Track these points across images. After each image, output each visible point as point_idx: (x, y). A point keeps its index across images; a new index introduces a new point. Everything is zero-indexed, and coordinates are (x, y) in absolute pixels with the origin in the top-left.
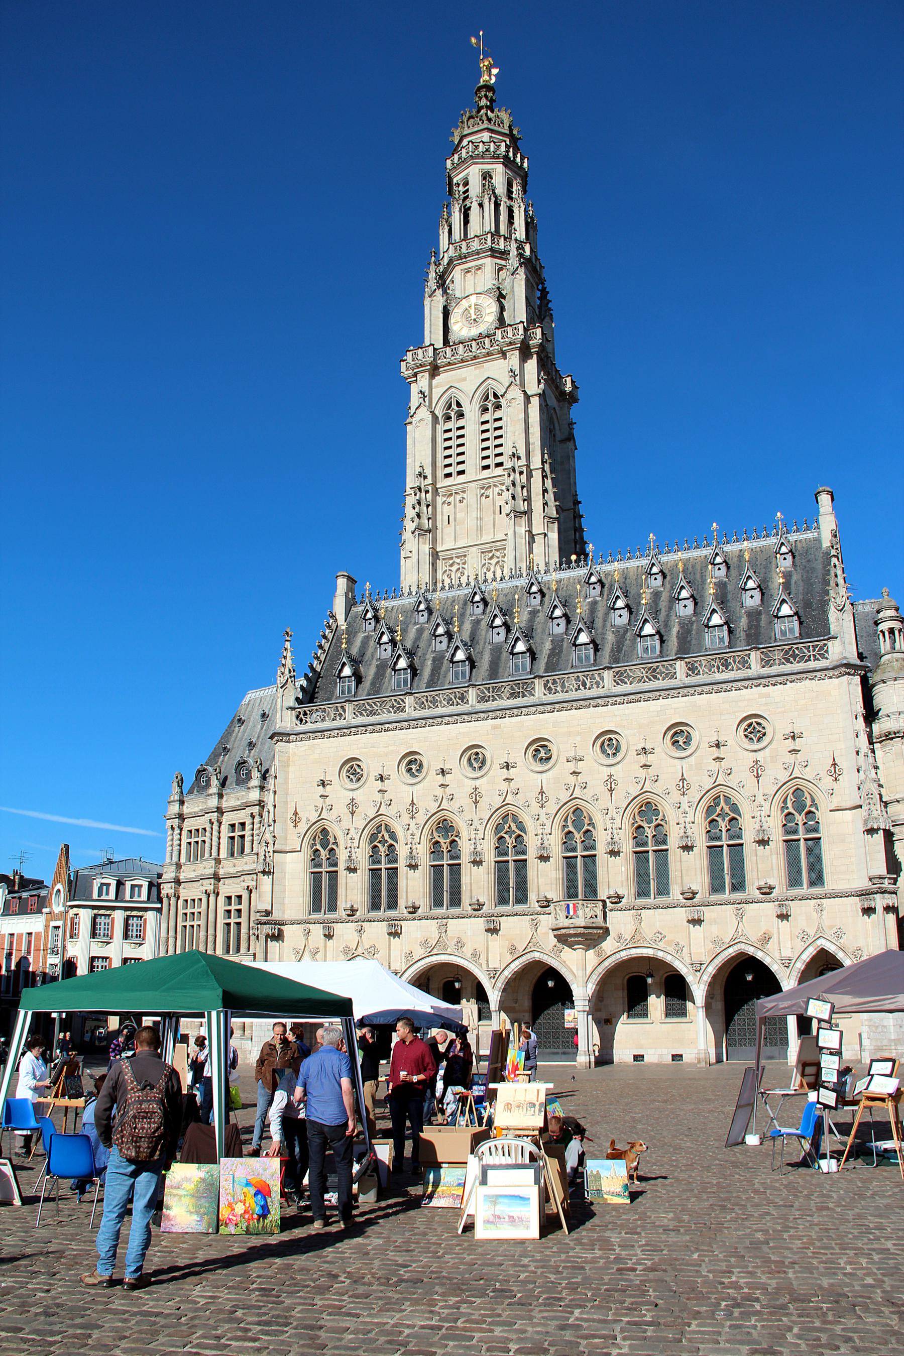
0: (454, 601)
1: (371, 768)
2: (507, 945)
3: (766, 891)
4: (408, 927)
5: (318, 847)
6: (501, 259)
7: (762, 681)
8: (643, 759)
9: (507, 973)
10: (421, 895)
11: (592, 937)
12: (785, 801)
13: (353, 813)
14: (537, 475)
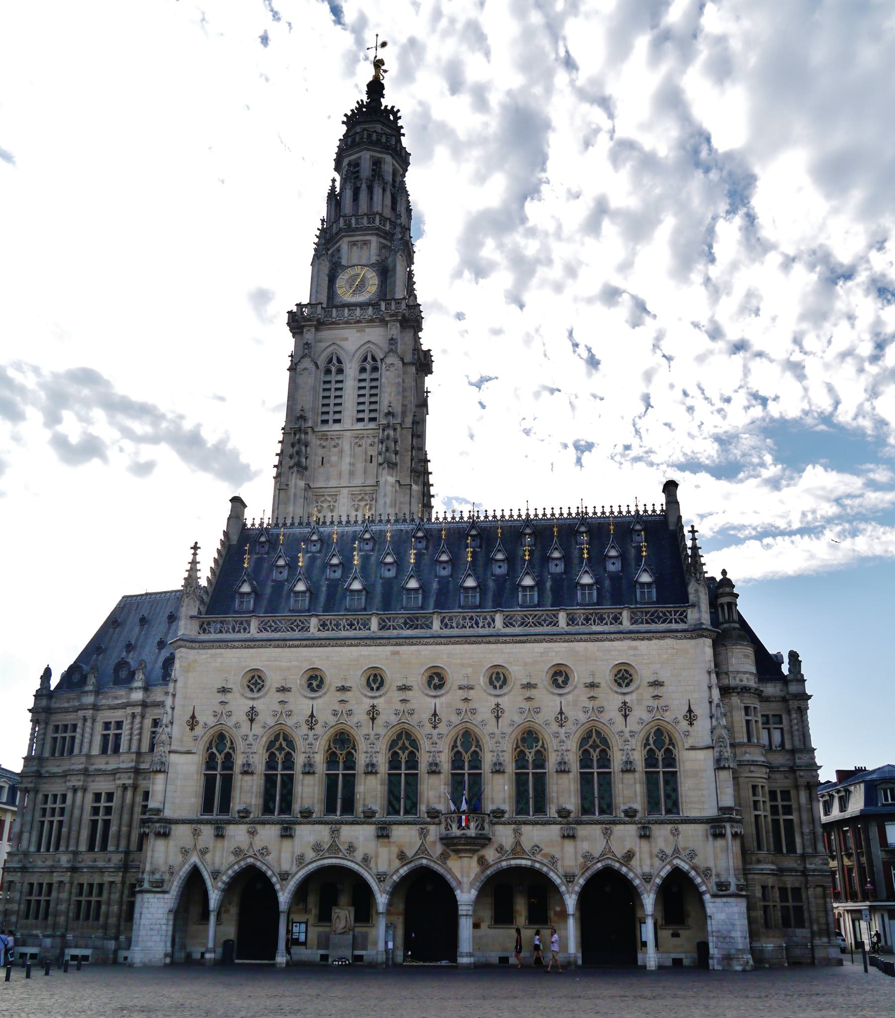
0: (343, 536)
2: (395, 850)
3: (631, 814)
5: (214, 750)
6: (385, 238)
7: (632, 635)
9: (395, 878)
10: (316, 801)
12: (647, 740)
13: (252, 720)
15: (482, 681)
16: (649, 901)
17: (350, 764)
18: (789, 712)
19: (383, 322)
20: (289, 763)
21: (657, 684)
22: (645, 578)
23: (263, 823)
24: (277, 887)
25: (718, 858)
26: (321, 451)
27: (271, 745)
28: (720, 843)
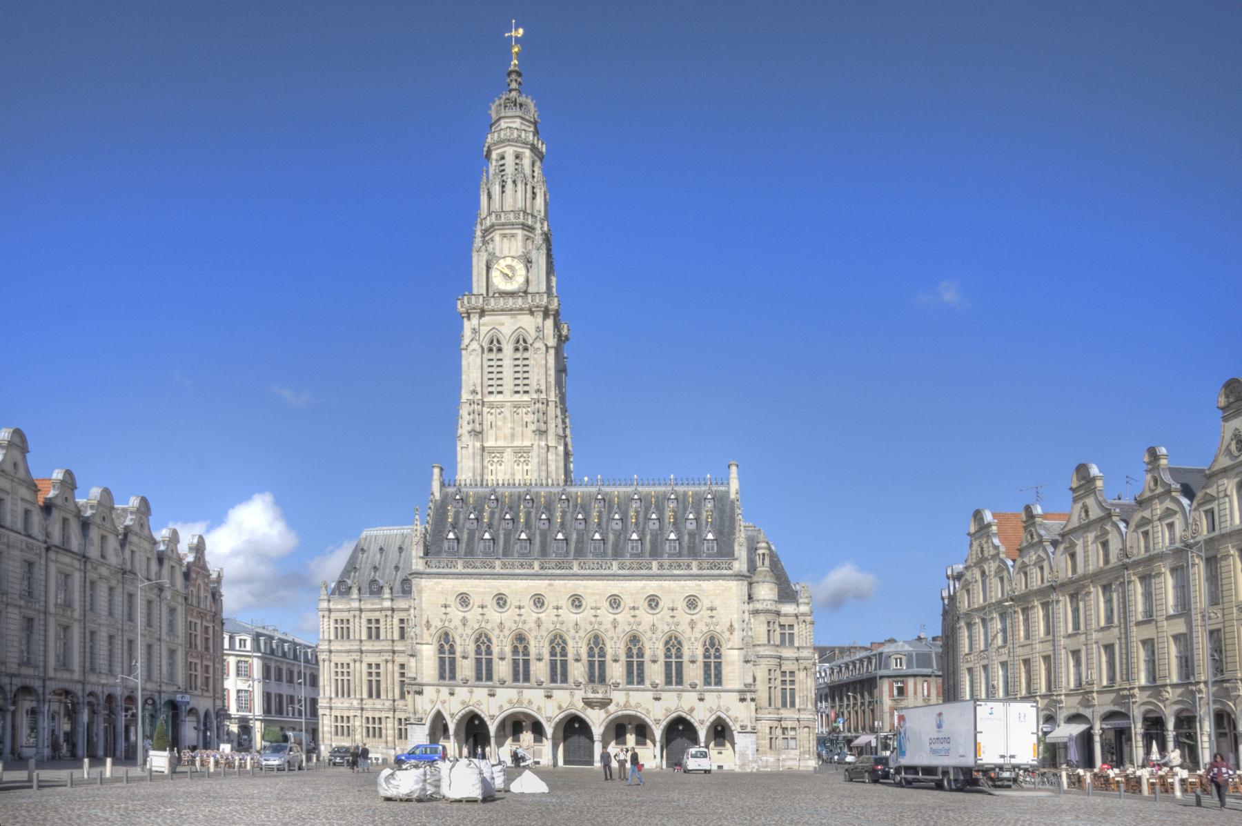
1: (475, 600)
3: (693, 686)
4: (499, 691)
8: (632, 612)
9: (557, 719)
11: (604, 704)
14: (552, 405)
17: (526, 653)
20: (489, 651)
21: (712, 609)
22: (710, 536)
24: (488, 723)
27: (477, 640)
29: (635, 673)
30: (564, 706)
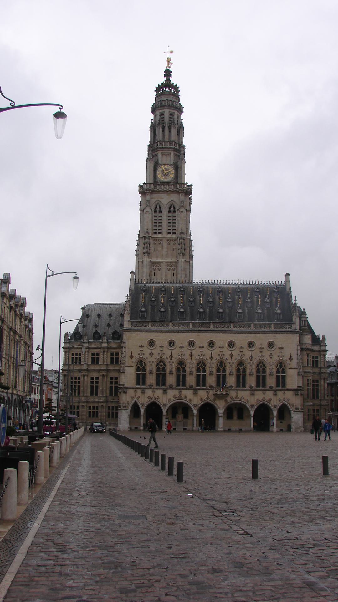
1: (158, 343)
2: (199, 397)
3: (271, 387)
13: (151, 356)
15: (226, 345)
16: (275, 413)
17: (184, 370)
18: (320, 355)
19: (178, 192)
23: (157, 389)
25: (296, 401)
26: (154, 246)
27: (158, 364)
28: (297, 397)
29: (241, 381)
30: (204, 399)
